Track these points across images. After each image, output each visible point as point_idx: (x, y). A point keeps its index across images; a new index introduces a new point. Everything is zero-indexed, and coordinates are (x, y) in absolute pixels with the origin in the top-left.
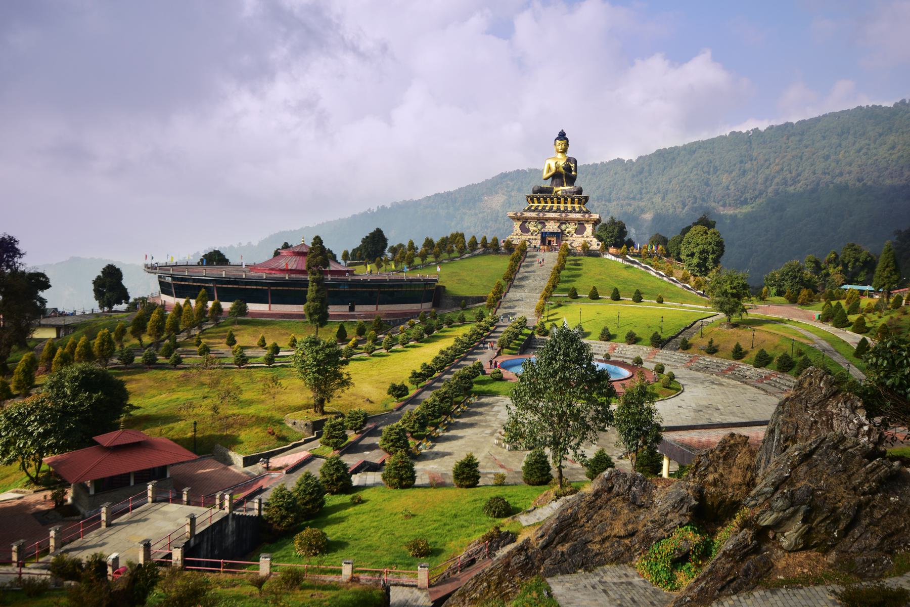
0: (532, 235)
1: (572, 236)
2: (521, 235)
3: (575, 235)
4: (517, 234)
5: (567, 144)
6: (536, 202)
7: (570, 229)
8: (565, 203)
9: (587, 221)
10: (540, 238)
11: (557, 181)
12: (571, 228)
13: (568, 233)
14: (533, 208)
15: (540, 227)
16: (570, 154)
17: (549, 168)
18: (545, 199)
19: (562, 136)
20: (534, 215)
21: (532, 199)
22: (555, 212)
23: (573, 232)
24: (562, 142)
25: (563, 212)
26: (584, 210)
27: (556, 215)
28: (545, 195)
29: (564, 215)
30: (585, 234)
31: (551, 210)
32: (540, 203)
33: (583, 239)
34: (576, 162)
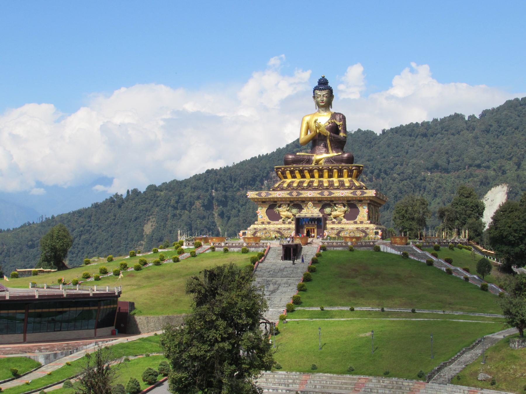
0: (284, 223)
1: (339, 223)
2: (269, 223)
3: (344, 220)
4: (263, 223)
5: (330, 95)
6: (289, 176)
8: (330, 176)
10: (293, 226)
12: (340, 211)
14: (285, 185)
16: (336, 108)
18: (301, 172)
19: (323, 84)
20: (284, 194)
21: (283, 173)
22: (315, 189)
23: (341, 217)
24: (324, 93)
25: (327, 189)
26: (357, 184)
28: (301, 167)
29: (326, 193)
30: (359, 218)
31: (310, 187)
32: (294, 177)
33: (356, 226)
34: (344, 119)
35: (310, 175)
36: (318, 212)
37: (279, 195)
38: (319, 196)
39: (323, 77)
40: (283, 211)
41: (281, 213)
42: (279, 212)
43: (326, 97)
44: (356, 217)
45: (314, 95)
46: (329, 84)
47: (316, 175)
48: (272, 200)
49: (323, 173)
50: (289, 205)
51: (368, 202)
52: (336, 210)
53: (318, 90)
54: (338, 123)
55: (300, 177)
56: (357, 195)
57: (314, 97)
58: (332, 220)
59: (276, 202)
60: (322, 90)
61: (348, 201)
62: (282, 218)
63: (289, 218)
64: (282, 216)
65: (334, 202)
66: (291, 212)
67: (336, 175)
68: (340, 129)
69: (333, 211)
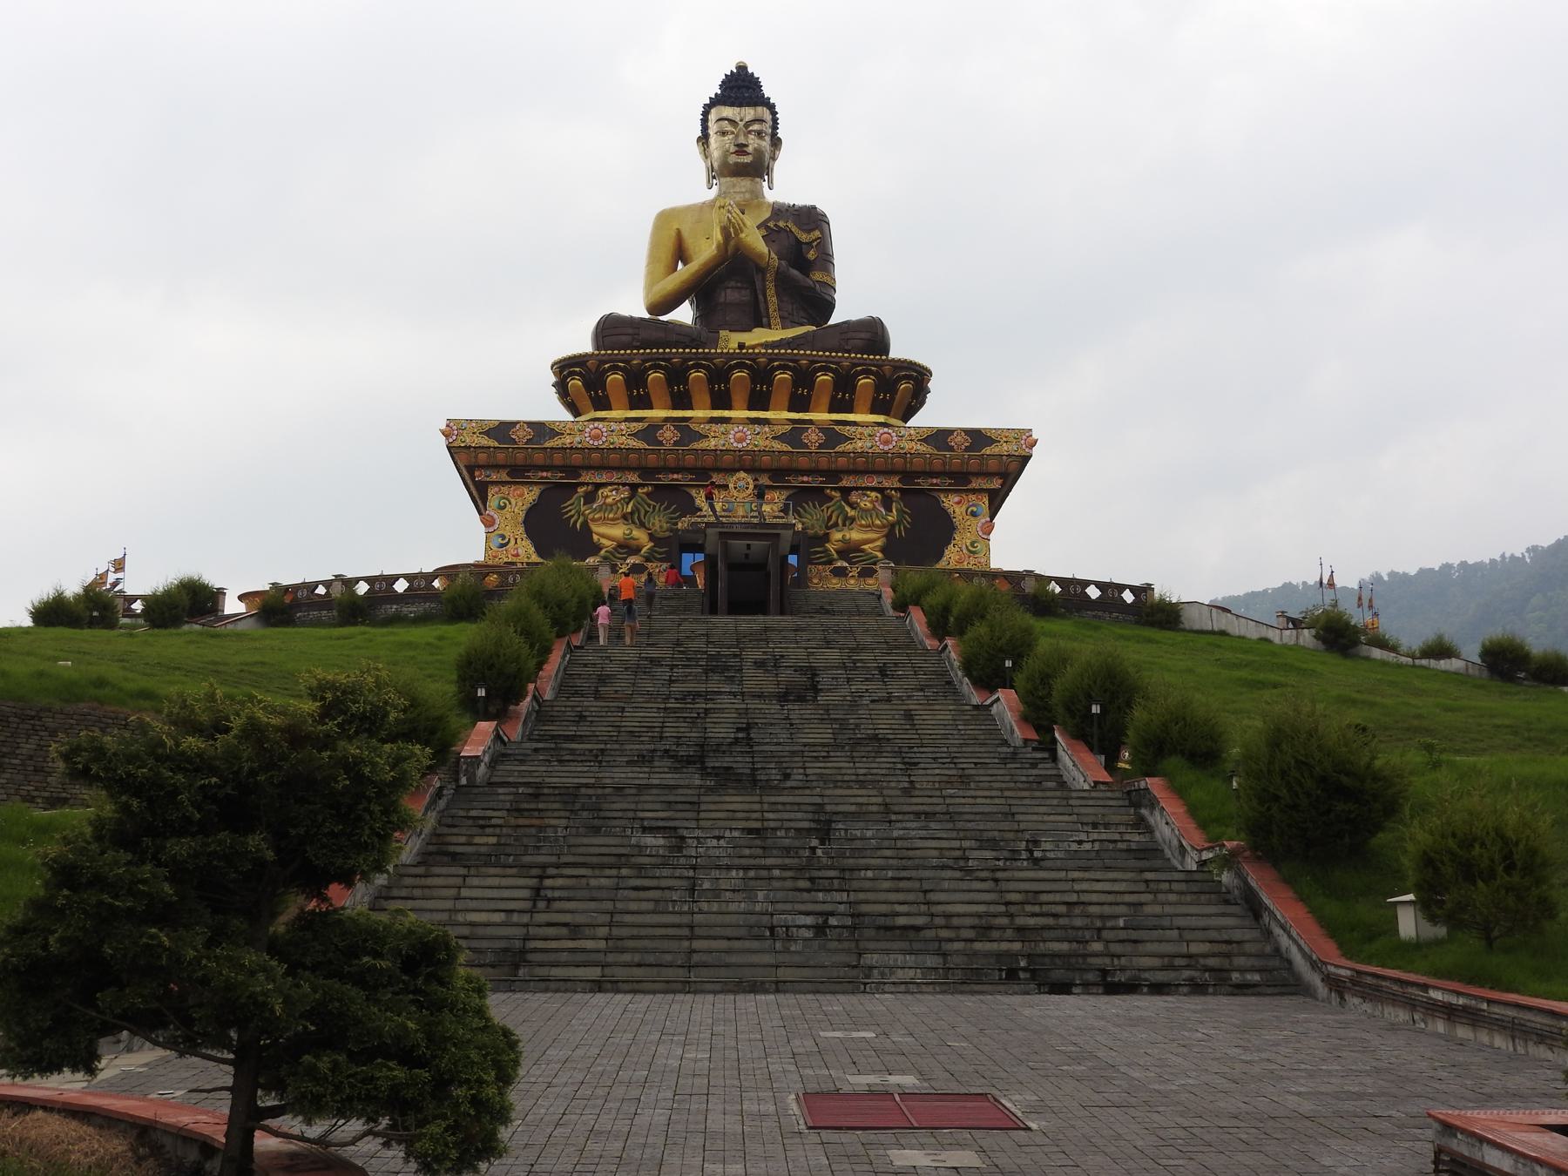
7: (855, 535)
9: (960, 480)
11: (731, 295)
13: (850, 551)
15: (659, 523)
17: (681, 253)
24: (749, 113)
27: (759, 440)
35: (712, 391)
36: (782, 514)
37: (597, 438)
38: (778, 446)
39: (742, 68)
40: (604, 521)
41: (594, 528)
42: (585, 525)
43: (759, 134)
44: (940, 555)
45: (705, 127)
46: (767, 91)
47: (739, 396)
48: (558, 459)
49: (770, 383)
50: (634, 487)
51: (996, 484)
52: (849, 521)
53: (725, 104)
54: (804, 237)
55: (669, 402)
56: (951, 449)
57: (704, 139)
58: (830, 562)
59: (574, 471)
60: (740, 106)
61: (907, 475)
62: (595, 549)
63: (636, 551)
64: (604, 541)
65: (845, 483)
66: (642, 525)
67: (825, 401)
68: (811, 255)
69: (836, 525)
